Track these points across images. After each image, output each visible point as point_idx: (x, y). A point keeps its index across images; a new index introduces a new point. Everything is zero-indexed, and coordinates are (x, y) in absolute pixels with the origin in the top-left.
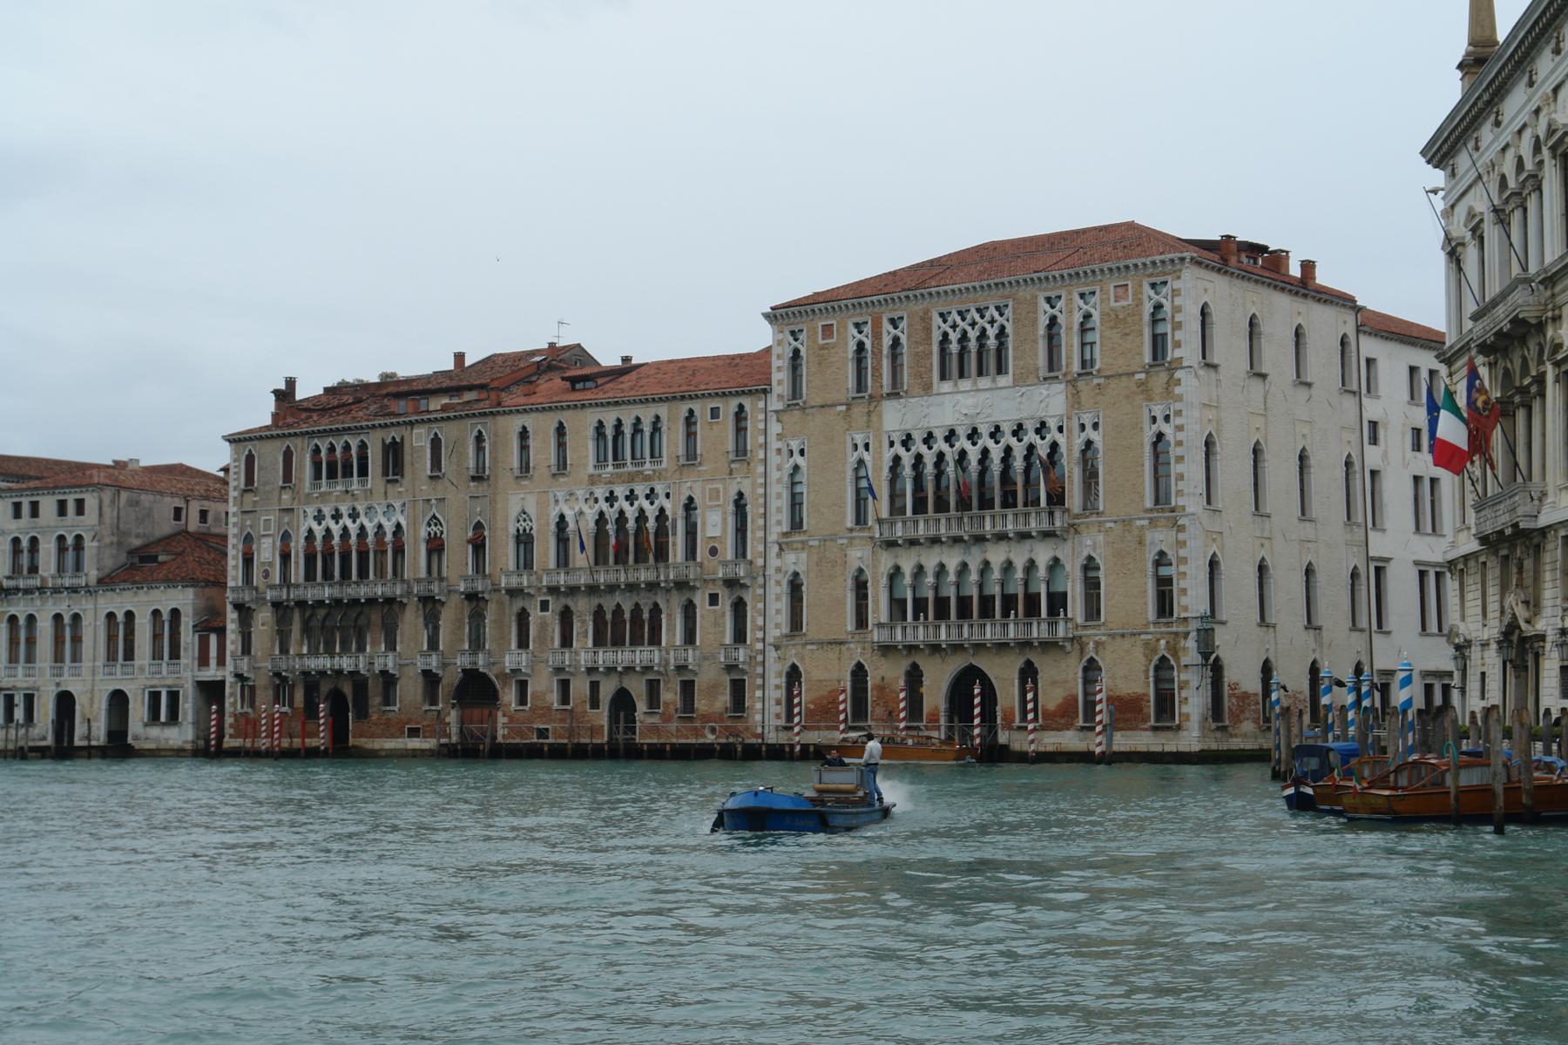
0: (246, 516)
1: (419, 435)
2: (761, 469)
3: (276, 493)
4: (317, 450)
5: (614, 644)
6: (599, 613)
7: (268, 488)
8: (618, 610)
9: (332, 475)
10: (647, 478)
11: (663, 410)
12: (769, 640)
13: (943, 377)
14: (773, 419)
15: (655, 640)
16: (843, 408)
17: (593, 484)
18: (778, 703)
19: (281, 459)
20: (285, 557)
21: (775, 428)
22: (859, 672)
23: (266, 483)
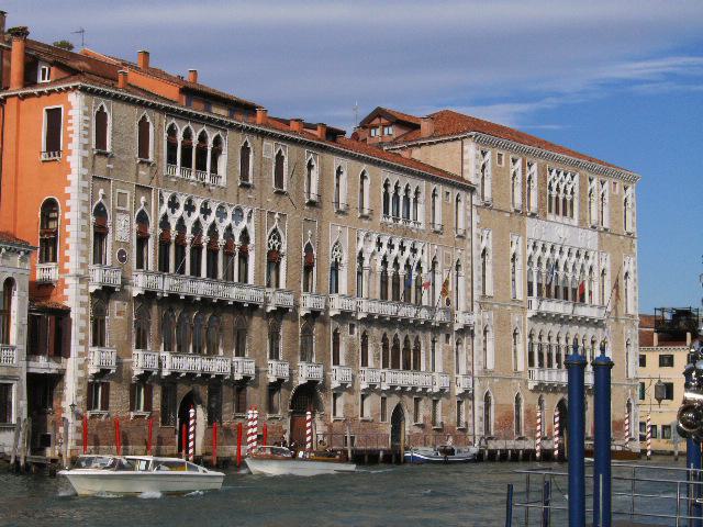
0: (97, 184)
1: (269, 147)
2: (469, 246)
3: (133, 166)
4: (172, 132)
5: (393, 367)
6: (385, 339)
7: (124, 158)
8: (396, 340)
9: (186, 163)
10: (413, 236)
11: (423, 184)
12: (476, 374)
13: (550, 211)
14: (474, 211)
15: (417, 367)
16: (508, 215)
17: (383, 230)
18: (481, 419)
19: (137, 129)
20: (142, 241)
21: (476, 219)
22: (518, 400)
23: (121, 151)
